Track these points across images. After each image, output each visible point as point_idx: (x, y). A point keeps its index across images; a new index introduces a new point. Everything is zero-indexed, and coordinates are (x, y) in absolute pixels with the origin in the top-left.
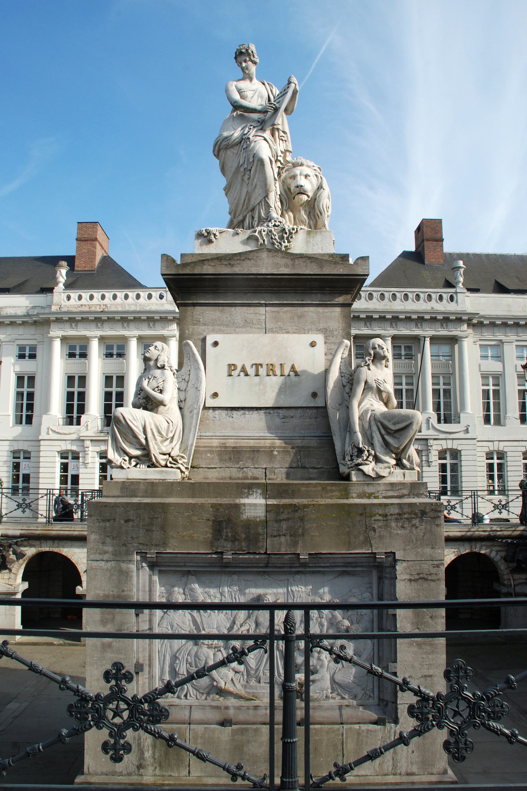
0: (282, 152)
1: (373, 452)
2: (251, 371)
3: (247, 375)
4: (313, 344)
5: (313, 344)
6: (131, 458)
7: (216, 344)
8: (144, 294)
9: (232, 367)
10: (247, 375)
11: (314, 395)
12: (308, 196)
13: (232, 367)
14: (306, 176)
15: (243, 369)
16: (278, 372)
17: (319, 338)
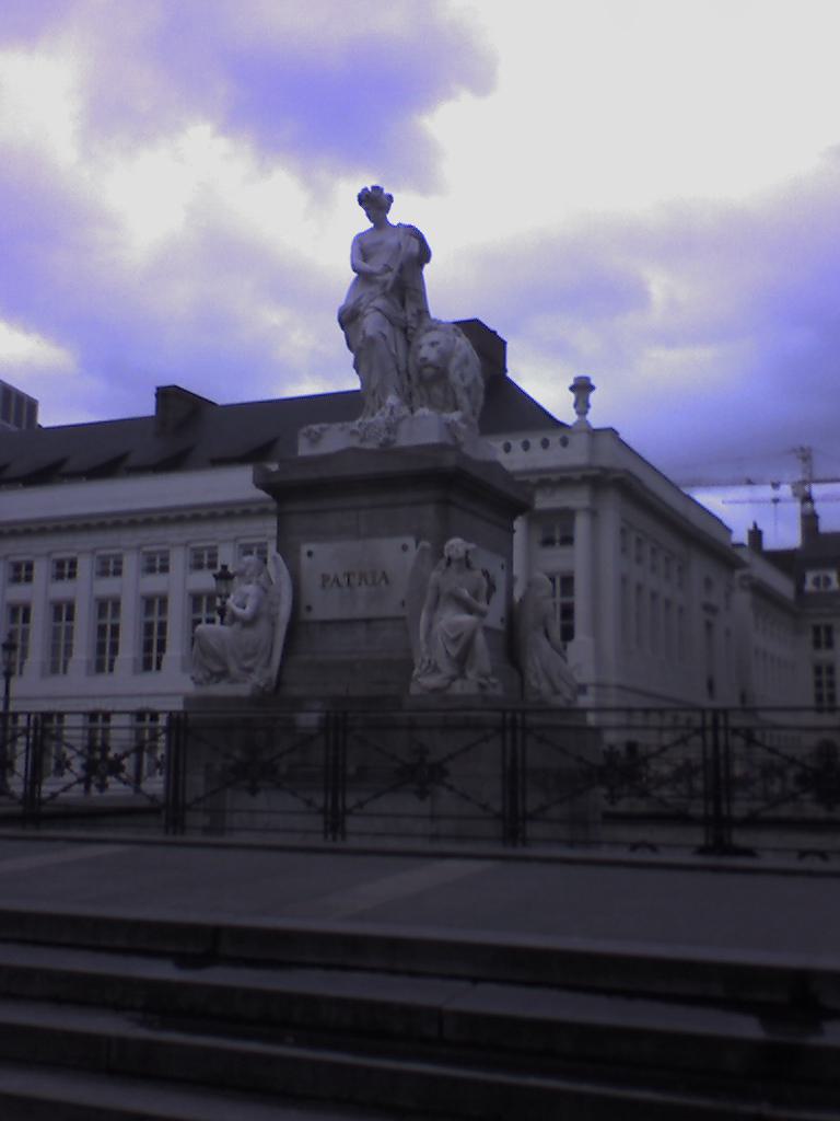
0: (413, 315)
1: (433, 662)
2: (343, 581)
3: (339, 585)
4: (405, 548)
5: (405, 548)
6: (213, 674)
7: (310, 554)
8: (554, 439)
9: (325, 578)
10: (339, 585)
11: (403, 604)
12: (438, 368)
13: (325, 578)
14: (433, 344)
15: (336, 580)
16: (370, 581)
17: (410, 541)
